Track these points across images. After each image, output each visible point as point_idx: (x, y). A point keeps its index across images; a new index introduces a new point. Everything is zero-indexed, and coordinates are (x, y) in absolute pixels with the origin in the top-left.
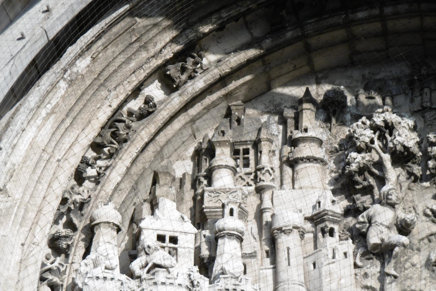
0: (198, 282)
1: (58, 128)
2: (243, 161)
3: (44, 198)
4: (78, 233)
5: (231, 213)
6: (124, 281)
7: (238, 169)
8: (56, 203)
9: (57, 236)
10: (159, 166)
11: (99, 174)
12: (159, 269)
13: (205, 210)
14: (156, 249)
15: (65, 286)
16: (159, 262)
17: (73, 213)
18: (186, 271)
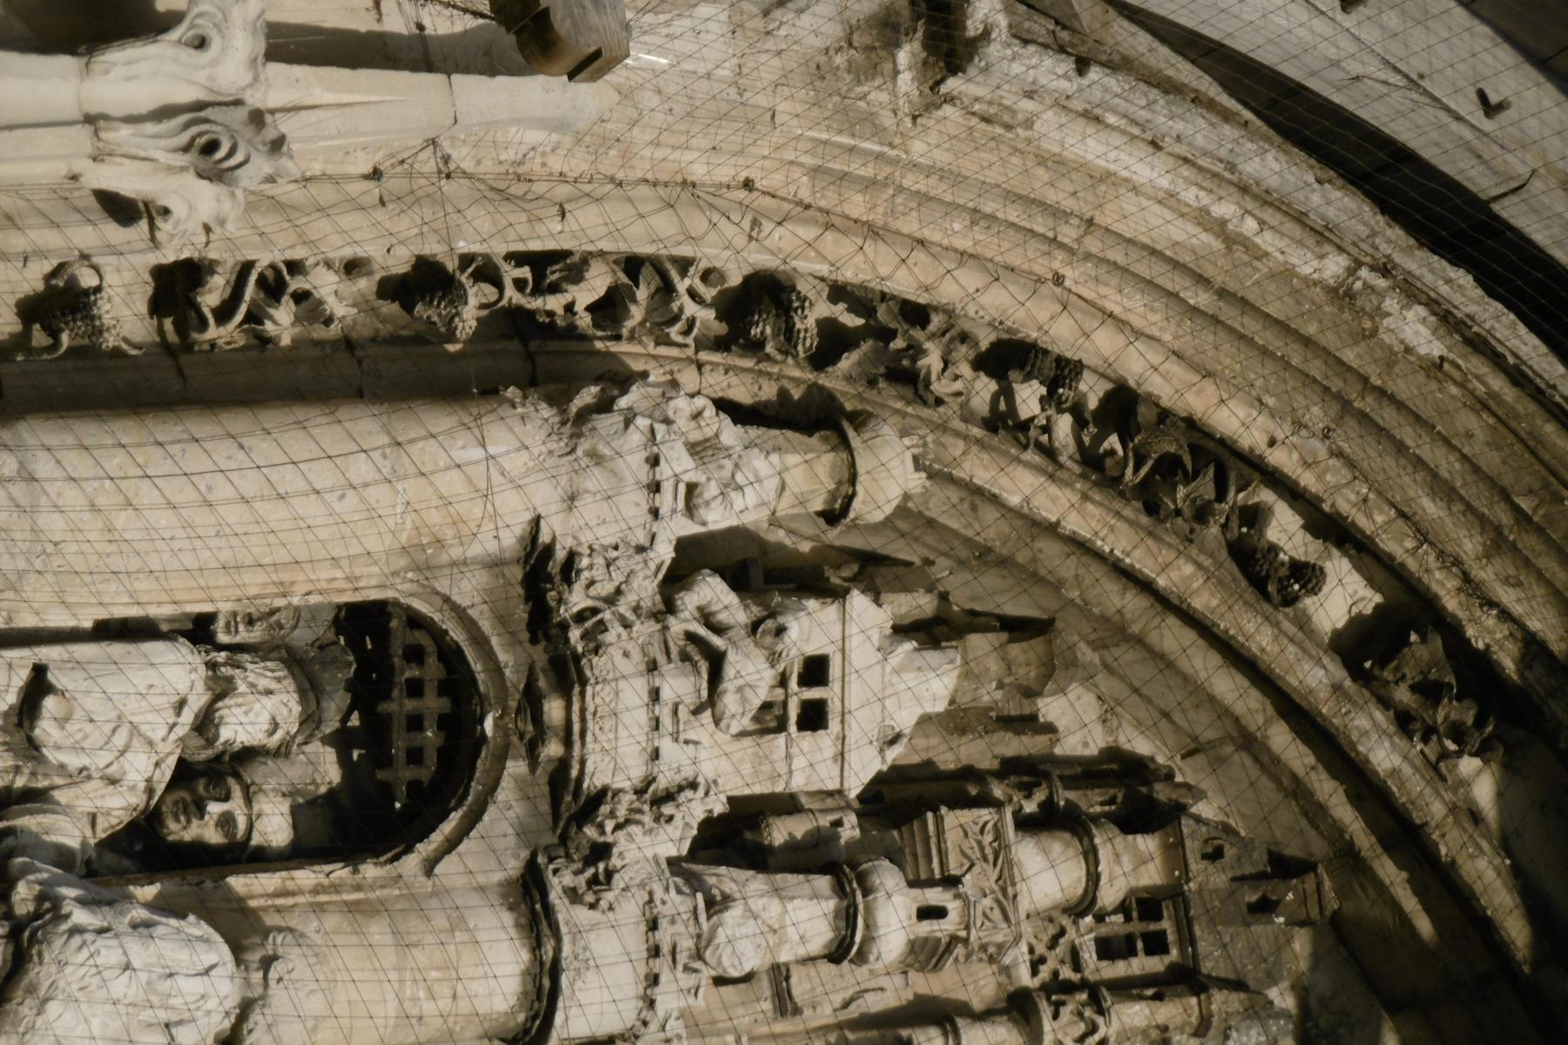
0: (670, 819)
1: (1176, 265)
2: (1117, 936)
3: (921, 242)
4: (809, 376)
6: (652, 554)
7: (1089, 919)
8: (905, 284)
9: (791, 302)
10: (1074, 637)
11: (1025, 426)
12: (705, 676)
13: (930, 815)
14: (773, 658)
15: (614, 347)
16: (729, 671)
17: (875, 351)
18: (707, 770)
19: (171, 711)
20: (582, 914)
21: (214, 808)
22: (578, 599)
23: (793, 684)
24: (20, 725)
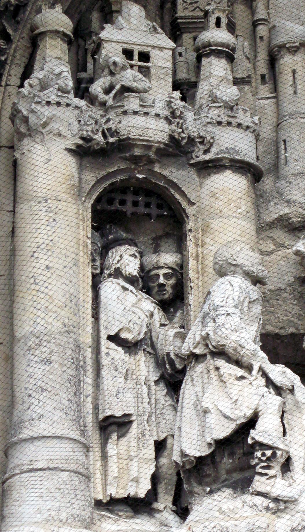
0: (181, 112)
5: (218, 24)
12: (130, 93)
13: (179, 21)
14: (124, 68)
17: (6, 20)
19: (126, 292)
20: (214, 150)
21: (162, 280)
22: (99, 137)
23: (133, 62)
24: (129, 347)
